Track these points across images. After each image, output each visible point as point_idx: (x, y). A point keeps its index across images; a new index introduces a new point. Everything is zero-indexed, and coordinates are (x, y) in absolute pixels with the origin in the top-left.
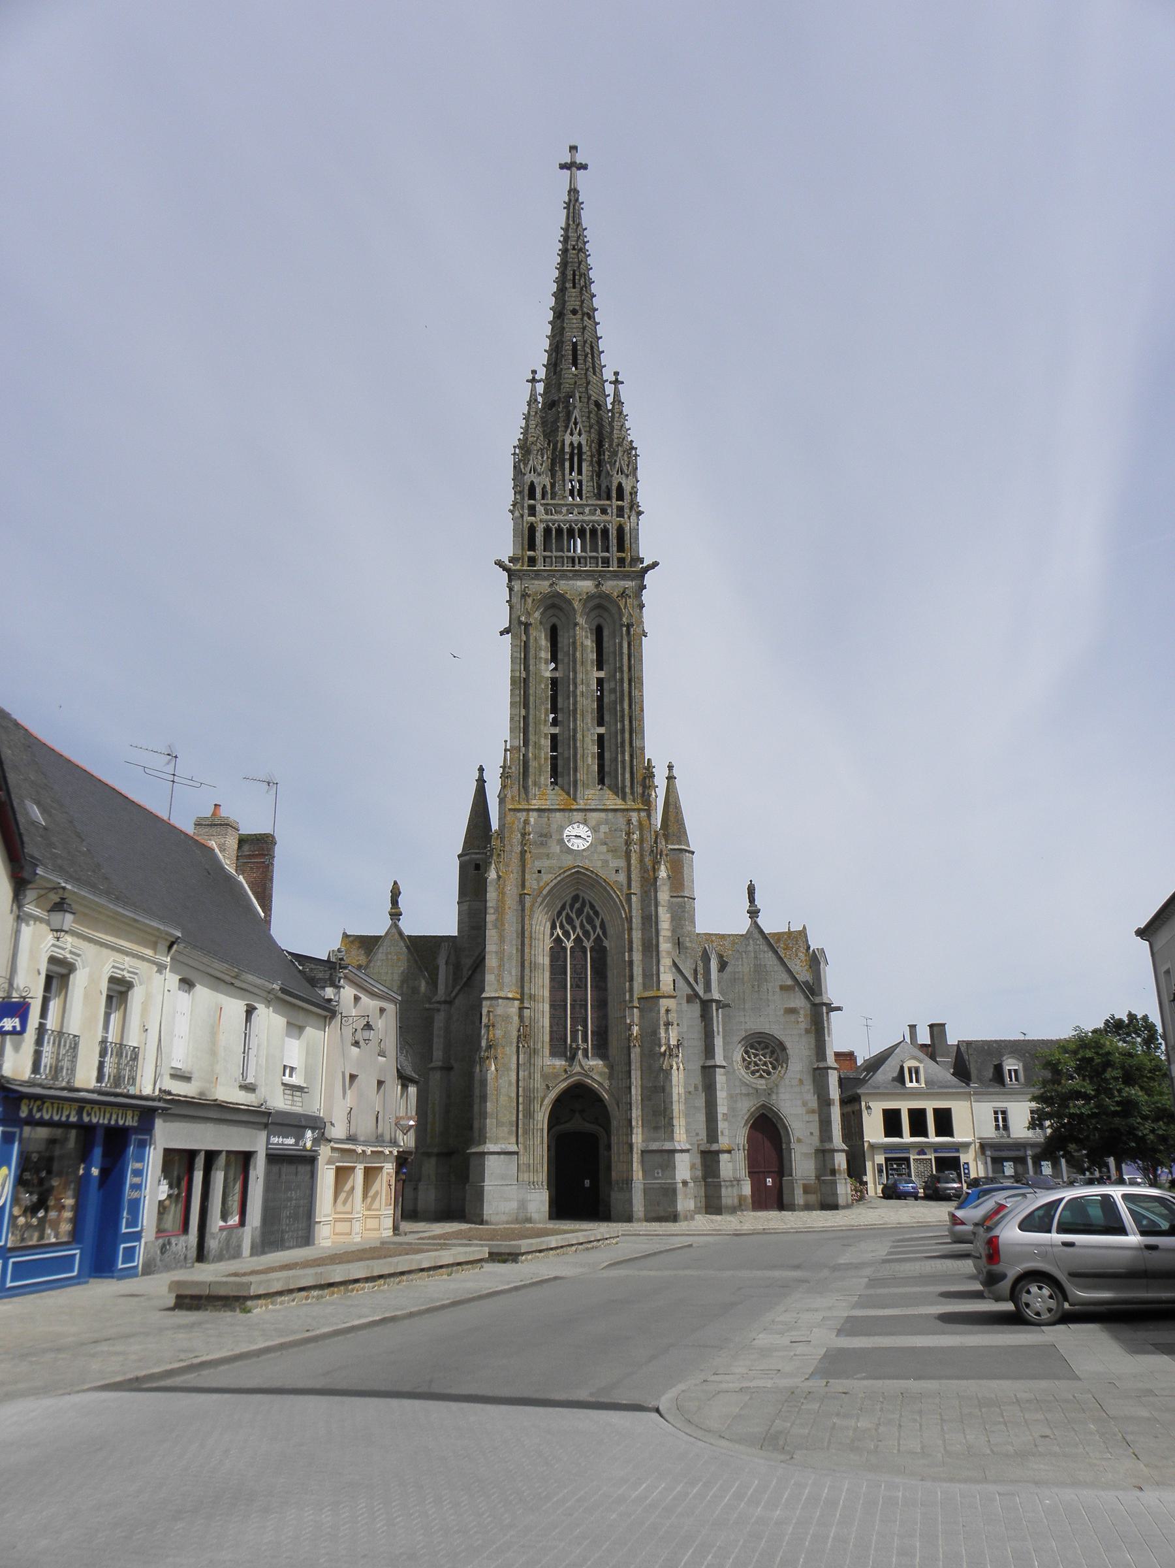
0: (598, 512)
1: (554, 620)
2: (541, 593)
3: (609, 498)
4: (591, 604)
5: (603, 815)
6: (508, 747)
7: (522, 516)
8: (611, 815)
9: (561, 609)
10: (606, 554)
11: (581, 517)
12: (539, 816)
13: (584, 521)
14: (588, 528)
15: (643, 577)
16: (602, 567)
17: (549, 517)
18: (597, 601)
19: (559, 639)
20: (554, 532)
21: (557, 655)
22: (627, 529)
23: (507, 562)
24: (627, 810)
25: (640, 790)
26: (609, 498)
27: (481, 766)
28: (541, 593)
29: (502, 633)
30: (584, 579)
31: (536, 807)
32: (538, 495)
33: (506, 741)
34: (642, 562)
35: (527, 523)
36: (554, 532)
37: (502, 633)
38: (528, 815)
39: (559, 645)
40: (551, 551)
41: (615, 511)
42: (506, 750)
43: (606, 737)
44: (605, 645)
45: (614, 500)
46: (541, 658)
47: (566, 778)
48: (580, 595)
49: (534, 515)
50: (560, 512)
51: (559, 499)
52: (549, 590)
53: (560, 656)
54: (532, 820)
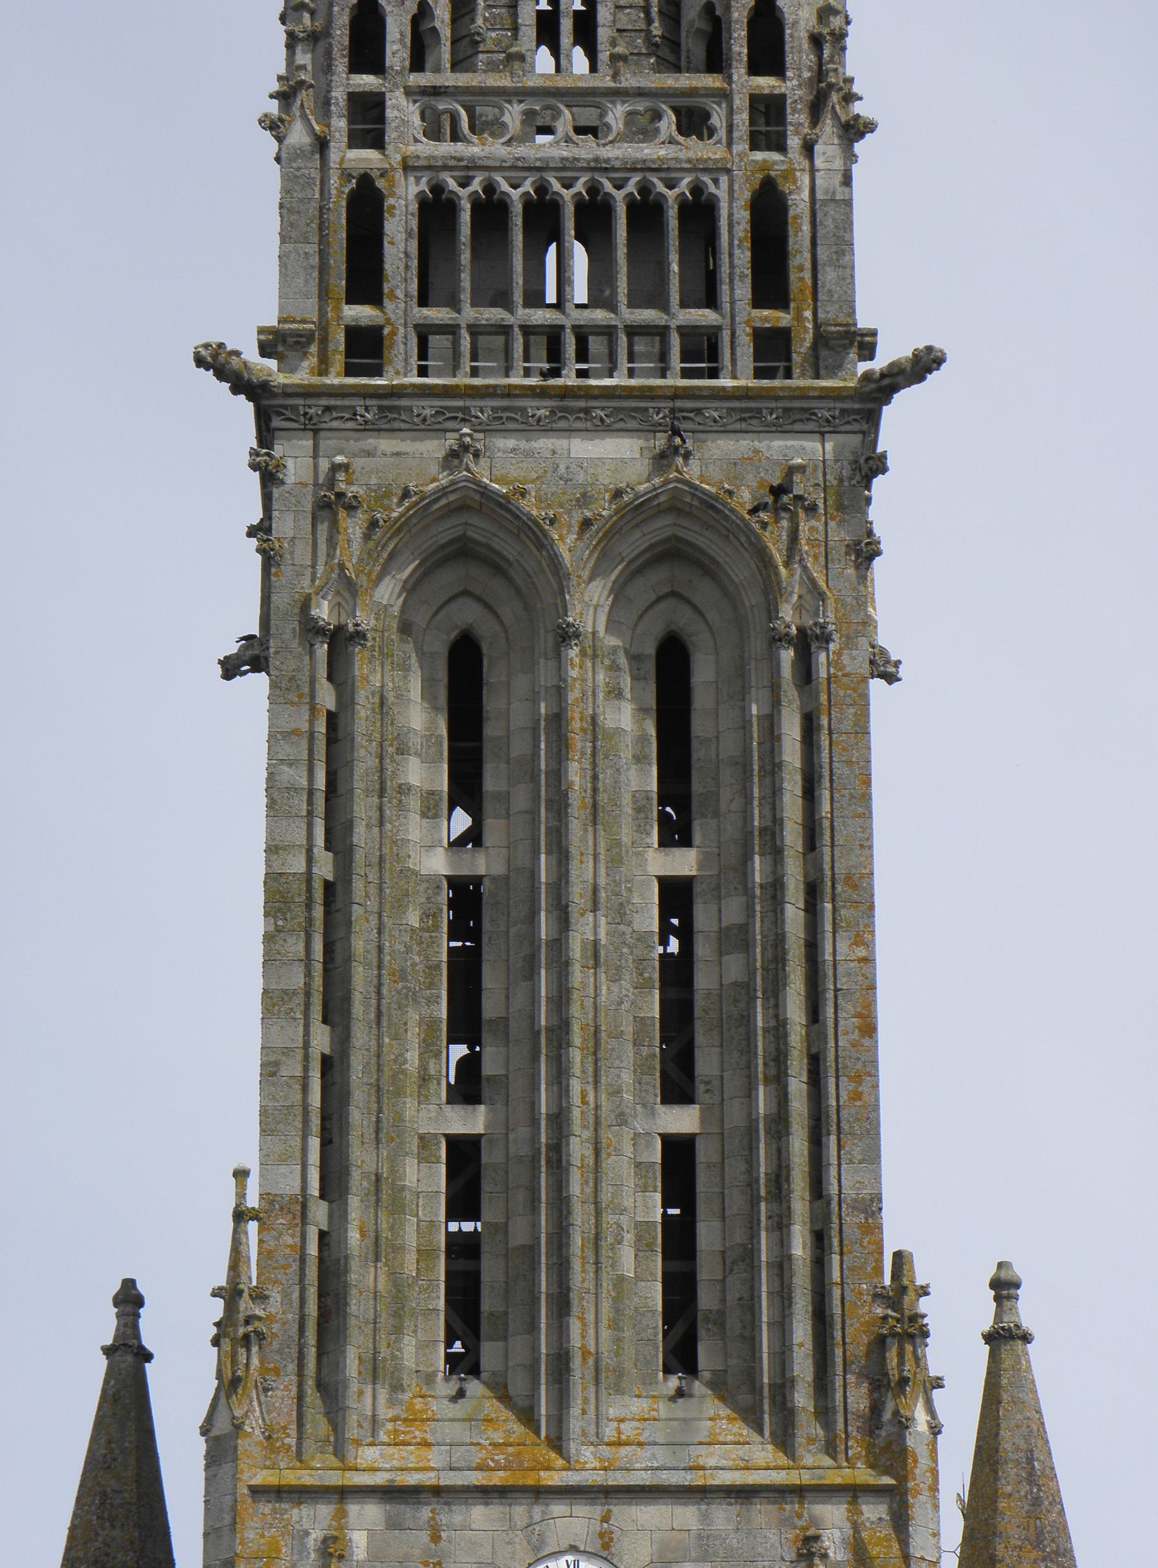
0: (668, 123)
1: (467, 614)
2: (406, 494)
3: (716, 61)
4: (634, 544)
5: (687, 1515)
6: (253, 1201)
7: (322, 144)
8: (722, 1515)
9: (498, 567)
10: (704, 316)
11: (587, 149)
12: (393, 1524)
13: (600, 167)
14: (619, 195)
15: (872, 419)
16: (686, 374)
17: (446, 149)
18: (660, 528)
19: (492, 704)
20: (465, 217)
21: (478, 775)
22: (799, 201)
23: (251, 354)
24: (800, 1492)
25: (858, 1398)
26: (716, 61)
27: (129, 1285)
28: (406, 494)
29: (230, 668)
30: (603, 428)
31: (380, 1479)
32: (396, 50)
33: (241, 1175)
34: (868, 350)
35: (346, 175)
36: (465, 217)
37: (230, 668)
38: (341, 1515)
39: (490, 730)
40: (454, 304)
41: (742, 119)
42: (240, 1216)
43: (704, 1154)
44: (700, 726)
45: (739, 72)
46: (404, 790)
47: (518, 1344)
48: (585, 499)
49: (378, 142)
50: (495, 127)
51: (492, 67)
52: (444, 479)
53: (492, 781)
54: (359, 1541)
